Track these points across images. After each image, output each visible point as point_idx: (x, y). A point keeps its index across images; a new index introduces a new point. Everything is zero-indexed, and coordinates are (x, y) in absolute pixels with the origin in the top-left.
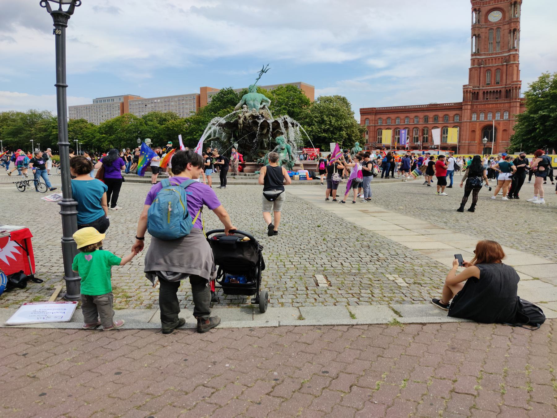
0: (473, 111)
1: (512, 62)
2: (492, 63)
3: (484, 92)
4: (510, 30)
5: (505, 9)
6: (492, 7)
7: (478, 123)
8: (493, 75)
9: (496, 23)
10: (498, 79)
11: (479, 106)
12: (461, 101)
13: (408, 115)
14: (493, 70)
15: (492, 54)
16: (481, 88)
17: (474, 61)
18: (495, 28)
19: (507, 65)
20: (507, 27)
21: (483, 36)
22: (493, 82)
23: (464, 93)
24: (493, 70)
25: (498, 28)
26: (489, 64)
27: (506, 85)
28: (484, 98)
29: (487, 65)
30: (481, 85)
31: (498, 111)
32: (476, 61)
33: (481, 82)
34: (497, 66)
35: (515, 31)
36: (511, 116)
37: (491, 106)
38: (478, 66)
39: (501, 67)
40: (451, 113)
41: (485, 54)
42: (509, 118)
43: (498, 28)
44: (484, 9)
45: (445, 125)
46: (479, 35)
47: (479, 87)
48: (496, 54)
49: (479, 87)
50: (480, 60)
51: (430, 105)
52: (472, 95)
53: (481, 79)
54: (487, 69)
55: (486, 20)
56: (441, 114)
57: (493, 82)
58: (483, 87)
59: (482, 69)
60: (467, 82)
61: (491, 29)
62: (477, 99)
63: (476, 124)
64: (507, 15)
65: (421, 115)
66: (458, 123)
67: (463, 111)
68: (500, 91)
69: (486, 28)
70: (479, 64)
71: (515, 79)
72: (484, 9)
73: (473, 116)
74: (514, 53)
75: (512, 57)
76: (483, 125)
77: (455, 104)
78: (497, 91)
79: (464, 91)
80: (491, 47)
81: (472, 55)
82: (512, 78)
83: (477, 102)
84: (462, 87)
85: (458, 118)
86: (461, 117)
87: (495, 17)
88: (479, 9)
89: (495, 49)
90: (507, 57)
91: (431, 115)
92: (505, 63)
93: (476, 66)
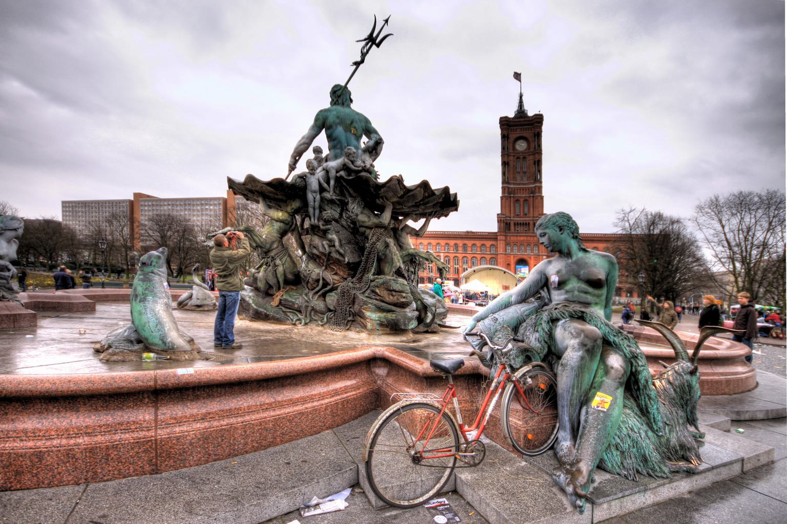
0: (507, 244)
1: (537, 194)
2: (520, 193)
3: (515, 223)
4: (535, 162)
5: (530, 139)
6: (518, 135)
7: (512, 256)
8: (522, 206)
9: (522, 152)
10: (526, 210)
11: (512, 238)
12: (496, 230)
13: (448, 241)
14: (522, 200)
15: (520, 184)
16: (512, 219)
17: (505, 189)
18: (522, 157)
19: (533, 197)
20: (531, 157)
21: (511, 163)
22: (522, 214)
23: (498, 222)
24: (522, 200)
25: (524, 158)
26: (517, 194)
27: (533, 217)
28: (515, 230)
29: (516, 195)
30: (512, 215)
31: (529, 245)
32: (507, 189)
33: (512, 212)
34: (525, 197)
35: (538, 163)
36: (540, 251)
37: (522, 238)
38: (509, 195)
39: (527, 198)
40: (488, 243)
41: (514, 184)
42: (539, 252)
43: (524, 158)
44: (513, 136)
45: (483, 256)
46: (508, 162)
47: (510, 217)
48: (523, 184)
49: (510, 217)
50: (510, 190)
51: (468, 232)
52: (505, 223)
53: (512, 208)
54: (516, 198)
55: (514, 148)
56: (478, 243)
57: (522, 214)
58: (514, 217)
59: (512, 199)
60: (500, 212)
61: (518, 158)
62: (509, 230)
63: (510, 257)
64: (532, 145)
65: (460, 243)
66: (494, 254)
67: (499, 242)
68: (529, 223)
69: (514, 156)
70: (509, 193)
71: (540, 213)
72: (513, 136)
73: (507, 248)
74: (539, 185)
75: (537, 188)
76: (516, 259)
77: (489, 233)
78: (526, 223)
79: (498, 221)
80: (518, 177)
81: (503, 183)
82: (539, 211)
83: (510, 233)
84: (496, 216)
85: (494, 249)
86: (497, 248)
87: (521, 146)
88: (508, 135)
89: (522, 180)
90: (533, 189)
91: (469, 243)
92: (532, 195)
93: (506, 195)
